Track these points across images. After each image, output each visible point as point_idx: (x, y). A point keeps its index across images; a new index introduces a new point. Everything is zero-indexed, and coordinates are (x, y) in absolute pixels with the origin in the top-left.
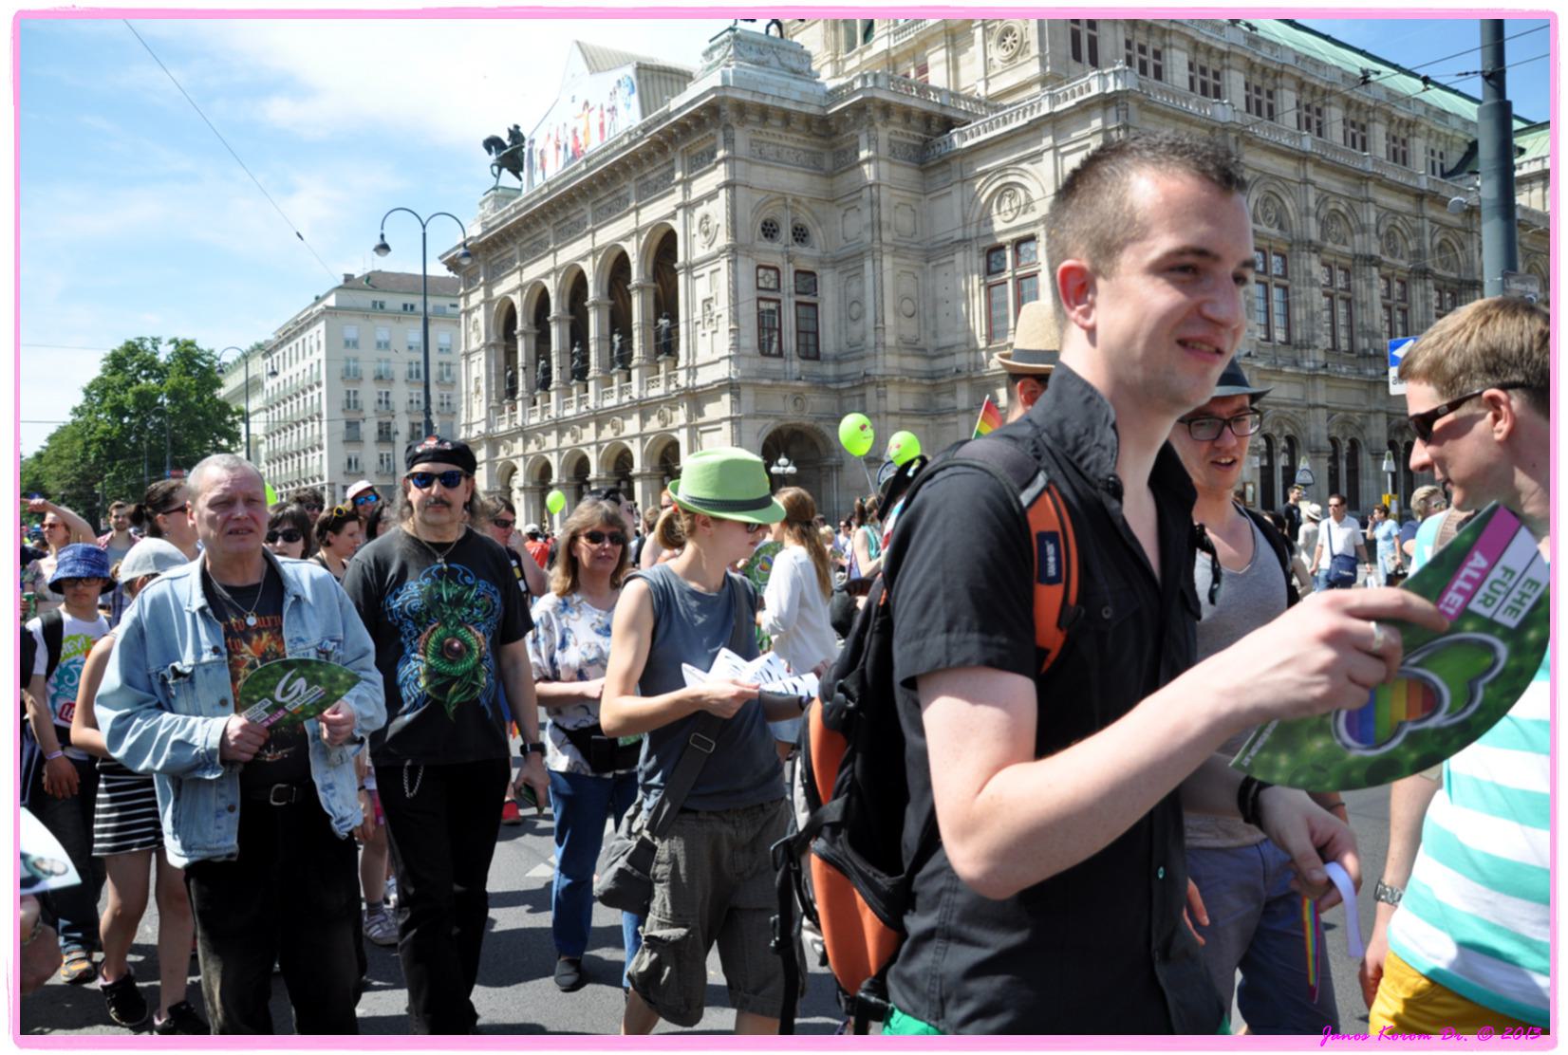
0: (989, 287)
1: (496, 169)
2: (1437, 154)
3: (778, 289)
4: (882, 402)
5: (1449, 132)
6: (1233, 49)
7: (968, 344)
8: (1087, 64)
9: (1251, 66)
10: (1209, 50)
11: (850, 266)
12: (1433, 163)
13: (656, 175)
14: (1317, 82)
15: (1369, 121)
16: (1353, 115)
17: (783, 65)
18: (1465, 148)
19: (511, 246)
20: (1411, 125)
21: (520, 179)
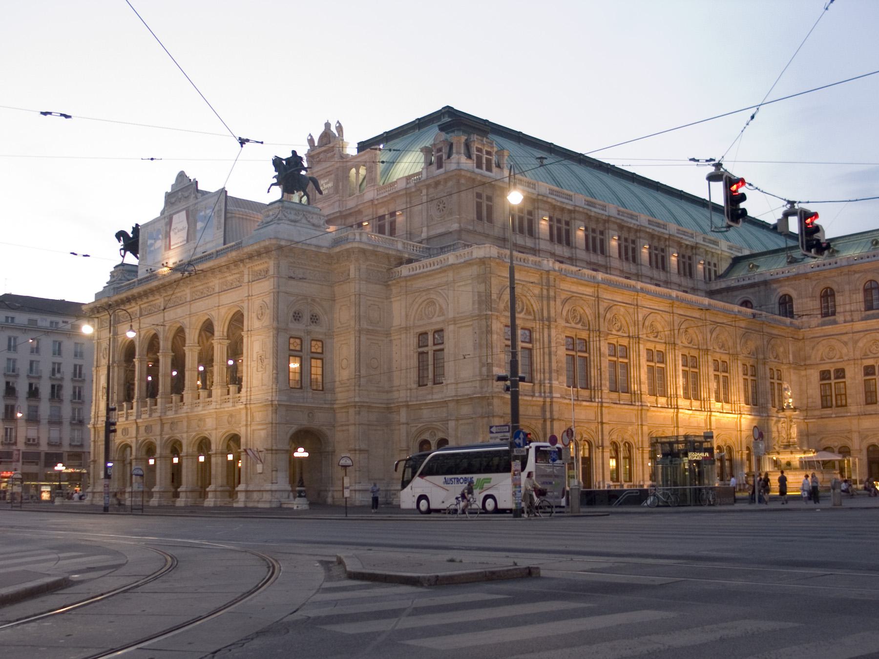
0: (420, 354)
1: (123, 252)
2: (712, 264)
3: (301, 351)
4: (357, 417)
5: (719, 252)
6: (577, 209)
7: (406, 385)
8: (486, 222)
9: (589, 217)
10: (562, 210)
11: (343, 338)
12: (709, 270)
13: (232, 277)
14: (632, 226)
15: (666, 246)
16: (655, 243)
17: (309, 221)
18: (730, 261)
19: (133, 304)
20: (694, 247)
21: (137, 258)
